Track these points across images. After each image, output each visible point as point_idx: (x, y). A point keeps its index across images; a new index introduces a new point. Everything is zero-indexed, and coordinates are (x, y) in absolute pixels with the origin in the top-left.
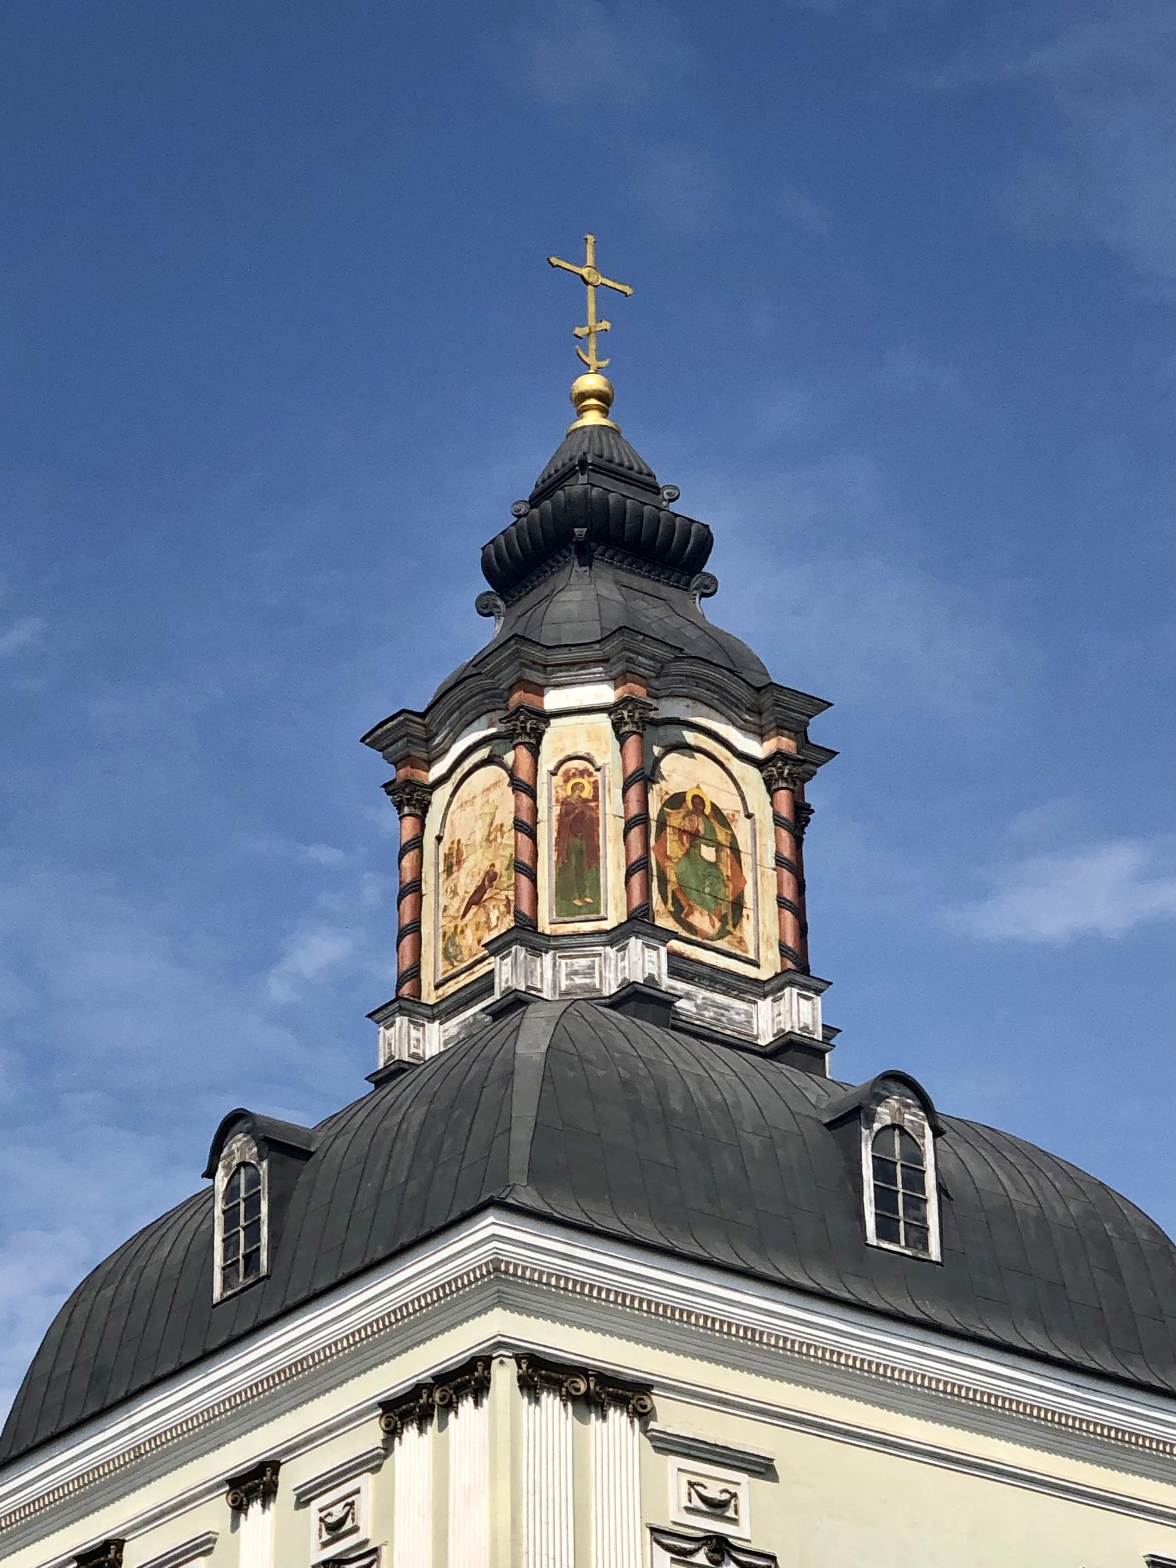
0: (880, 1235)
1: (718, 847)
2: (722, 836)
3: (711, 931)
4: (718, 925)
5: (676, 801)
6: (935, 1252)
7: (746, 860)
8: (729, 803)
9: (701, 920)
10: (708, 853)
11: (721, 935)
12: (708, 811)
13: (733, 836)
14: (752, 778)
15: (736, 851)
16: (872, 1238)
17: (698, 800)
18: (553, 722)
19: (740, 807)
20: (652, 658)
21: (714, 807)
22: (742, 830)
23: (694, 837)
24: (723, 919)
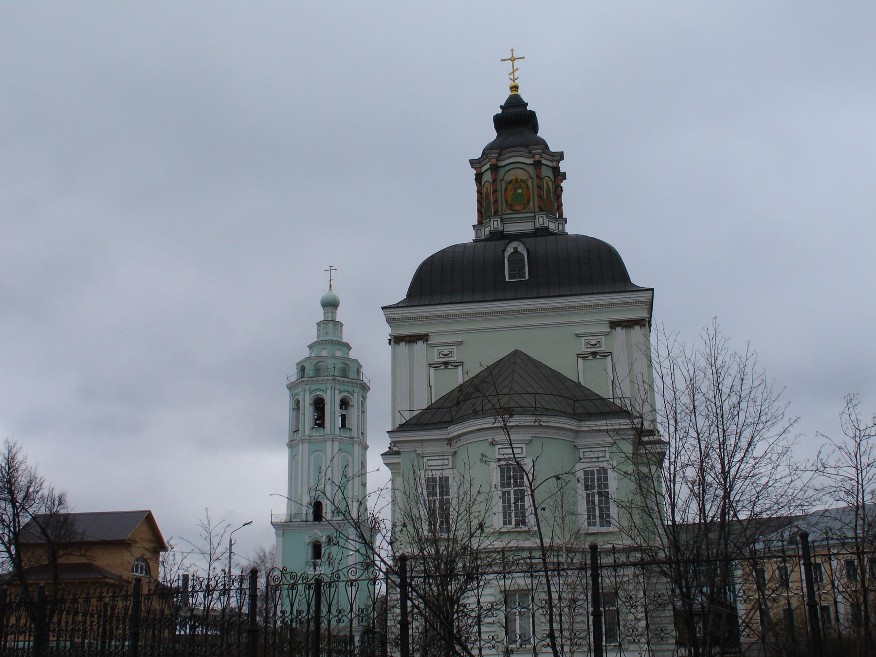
0: (509, 279)
1: (523, 189)
2: (523, 185)
3: (521, 209)
4: (522, 206)
5: (511, 182)
6: (527, 278)
7: (531, 189)
8: (524, 178)
9: (518, 208)
10: (519, 191)
11: (523, 209)
12: (519, 181)
13: (527, 185)
14: (531, 170)
15: (528, 187)
16: (507, 280)
17: (516, 180)
18: (484, 175)
19: (528, 177)
20: (495, 153)
21: (521, 179)
22: (530, 183)
23: (516, 189)
24: (524, 206)
